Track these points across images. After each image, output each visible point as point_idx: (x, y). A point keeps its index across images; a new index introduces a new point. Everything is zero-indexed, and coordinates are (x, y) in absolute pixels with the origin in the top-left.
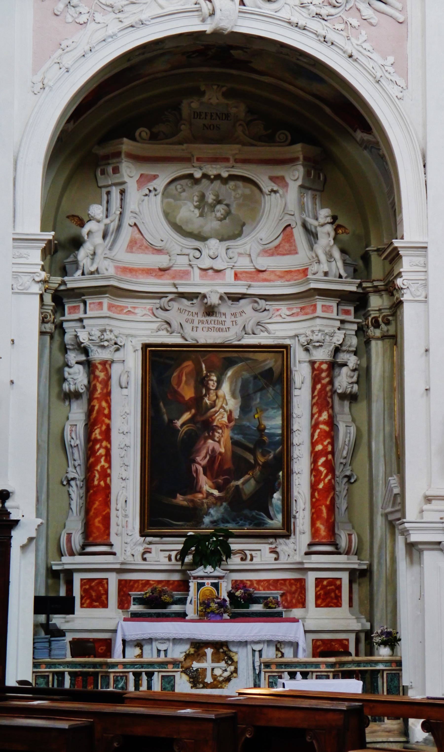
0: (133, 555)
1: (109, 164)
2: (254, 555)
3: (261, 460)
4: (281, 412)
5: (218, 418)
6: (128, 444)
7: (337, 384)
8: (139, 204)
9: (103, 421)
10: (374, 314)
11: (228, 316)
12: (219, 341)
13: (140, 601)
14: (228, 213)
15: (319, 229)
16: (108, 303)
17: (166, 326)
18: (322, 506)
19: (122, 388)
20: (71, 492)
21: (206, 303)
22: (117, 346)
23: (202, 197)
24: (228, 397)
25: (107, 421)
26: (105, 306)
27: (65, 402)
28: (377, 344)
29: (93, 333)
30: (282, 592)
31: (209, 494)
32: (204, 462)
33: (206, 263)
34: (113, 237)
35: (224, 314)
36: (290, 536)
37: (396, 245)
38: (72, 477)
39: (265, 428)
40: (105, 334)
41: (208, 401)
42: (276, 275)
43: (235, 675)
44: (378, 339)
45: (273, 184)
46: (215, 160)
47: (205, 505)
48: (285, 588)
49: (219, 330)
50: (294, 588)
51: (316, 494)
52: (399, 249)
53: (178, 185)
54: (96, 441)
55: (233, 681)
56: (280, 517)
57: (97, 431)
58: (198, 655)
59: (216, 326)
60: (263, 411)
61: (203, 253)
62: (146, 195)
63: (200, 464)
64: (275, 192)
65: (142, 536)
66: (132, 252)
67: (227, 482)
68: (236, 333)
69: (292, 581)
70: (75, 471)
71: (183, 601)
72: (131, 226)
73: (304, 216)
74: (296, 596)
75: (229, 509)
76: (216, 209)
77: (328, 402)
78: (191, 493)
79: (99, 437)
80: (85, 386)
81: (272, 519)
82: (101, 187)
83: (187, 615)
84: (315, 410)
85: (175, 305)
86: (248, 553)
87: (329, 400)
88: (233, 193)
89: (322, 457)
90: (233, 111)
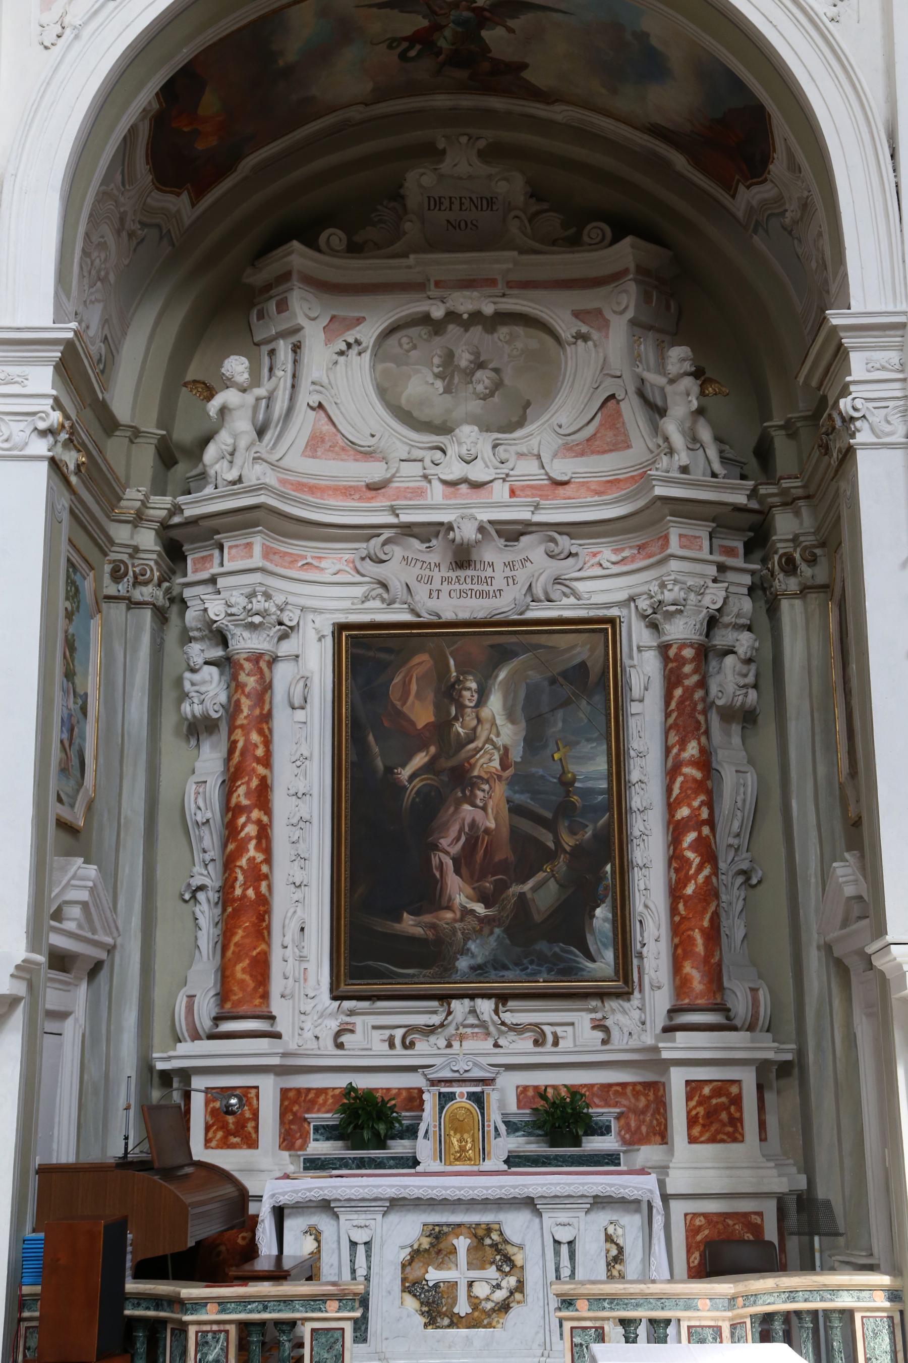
0: (317, 1038)
1: (271, 298)
2: (560, 1034)
3: (568, 841)
4: (605, 747)
5: (482, 761)
6: (306, 816)
7: (714, 689)
8: (329, 369)
9: (254, 770)
10: (782, 548)
11: (499, 566)
12: (480, 615)
13: (329, 1132)
14: (498, 385)
15: (669, 389)
16: (263, 544)
17: (380, 591)
18: (693, 930)
19: (293, 708)
20: (199, 915)
21: (454, 541)
22: (283, 627)
23: (449, 356)
24: (500, 720)
25: (261, 770)
26: (257, 550)
27: (188, 741)
28: (792, 606)
29: (233, 600)
30: (618, 1110)
31: (467, 912)
32: (456, 849)
33: (454, 470)
34: (278, 429)
35: (491, 565)
36: (632, 993)
37: (835, 321)
38: (199, 883)
39: (574, 780)
40: (254, 600)
41: (460, 730)
42: (589, 489)
43: (518, 1296)
44: (794, 596)
45: (580, 323)
46: (468, 284)
47: (459, 934)
48: (625, 1102)
49: (482, 594)
50: (642, 1102)
51: (681, 906)
52: (842, 334)
53: (402, 338)
54: (239, 810)
55: (516, 1311)
56: (609, 955)
57: (242, 790)
58: (439, 1252)
59: (476, 587)
60: (571, 745)
61: (449, 453)
62: (341, 353)
63: (447, 853)
64: (585, 338)
65: (334, 998)
66: (314, 457)
67: (500, 887)
68: (515, 599)
69: (639, 1088)
70: (205, 873)
71: (411, 1132)
72: (313, 409)
73: (639, 370)
74: (648, 1119)
75: (507, 941)
76: (474, 379)
77: (698, 722)
78: (430, 912)
79: (245, 802)
80: (222, 706)
81: (593, 960)
82: (257, 345)
83: (418, 1163)
84: (673, 738)
85: (397, 552)
86: (548, 1029)
87: (701, 718)
88: (507, 349)
89: (689, 831)
90: (501, 188)
